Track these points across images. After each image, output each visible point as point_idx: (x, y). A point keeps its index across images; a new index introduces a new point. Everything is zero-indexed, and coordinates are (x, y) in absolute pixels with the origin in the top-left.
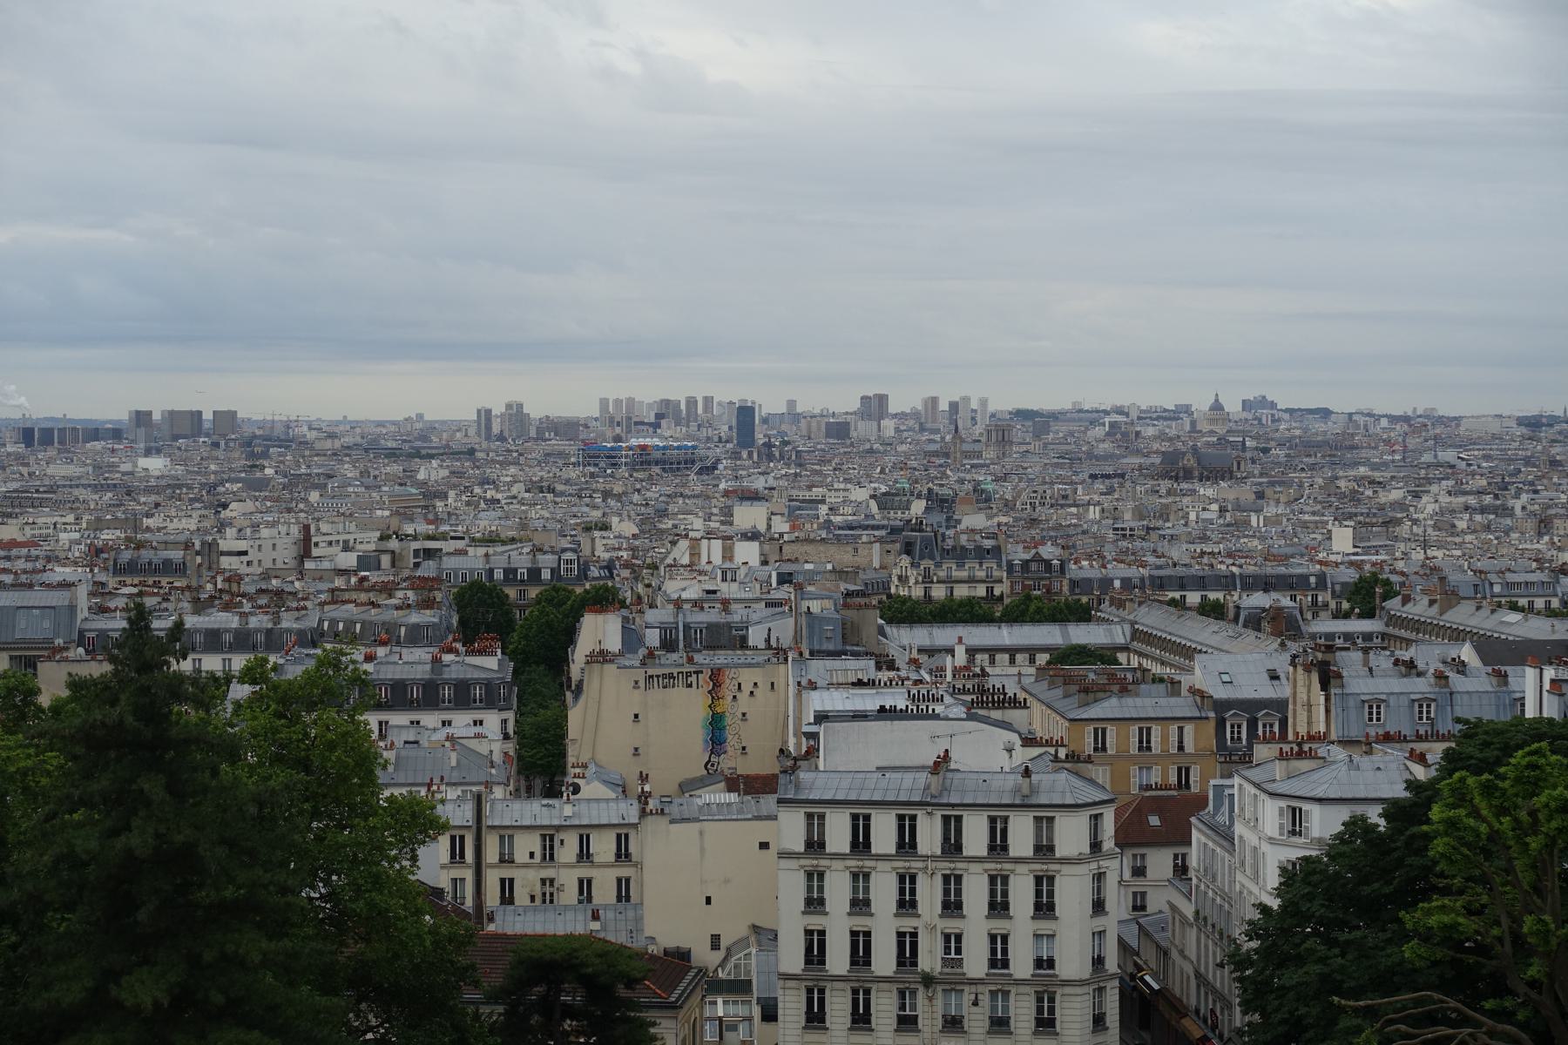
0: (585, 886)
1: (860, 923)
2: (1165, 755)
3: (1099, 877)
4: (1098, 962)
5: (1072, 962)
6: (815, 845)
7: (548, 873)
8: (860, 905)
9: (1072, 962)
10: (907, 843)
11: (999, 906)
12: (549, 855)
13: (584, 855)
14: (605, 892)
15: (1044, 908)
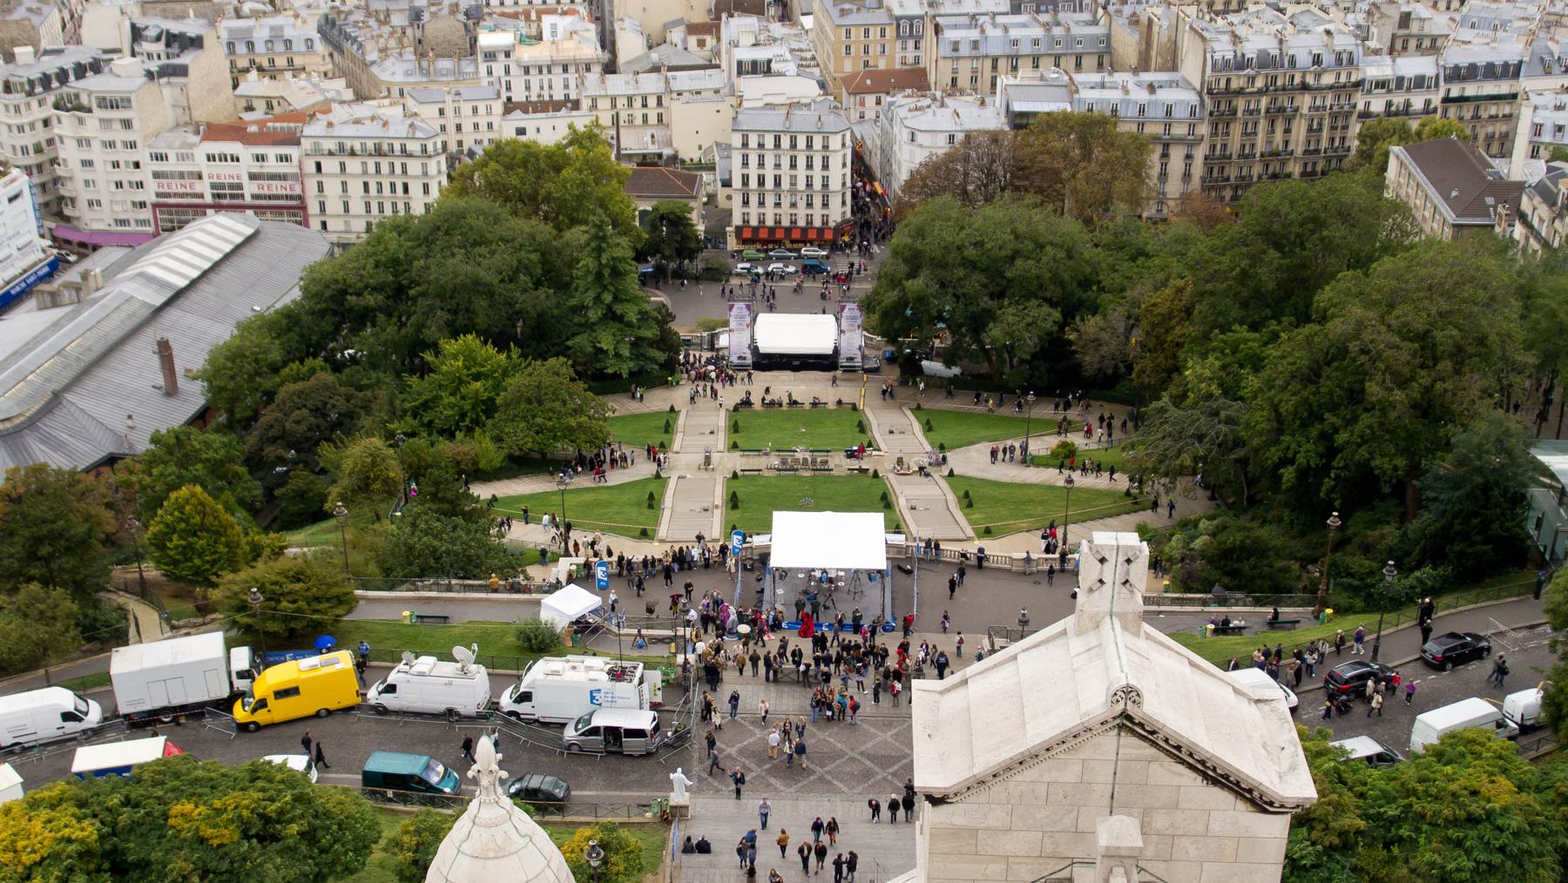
0: (645, 118)
1: (761, 172)
2: (875, 41)
3: (845, 155)
4: (844, 184)
5: (835, 184)
6: (745, 145)
7: (630, 112)
8: (761, 165)
9: (835, 184)
10: (777, 145)
11: (810, 166)
12: (630, 105)
13: (645, 105)
14: (653, 119)
15: (825, 167)
